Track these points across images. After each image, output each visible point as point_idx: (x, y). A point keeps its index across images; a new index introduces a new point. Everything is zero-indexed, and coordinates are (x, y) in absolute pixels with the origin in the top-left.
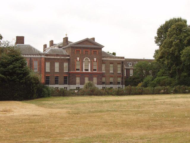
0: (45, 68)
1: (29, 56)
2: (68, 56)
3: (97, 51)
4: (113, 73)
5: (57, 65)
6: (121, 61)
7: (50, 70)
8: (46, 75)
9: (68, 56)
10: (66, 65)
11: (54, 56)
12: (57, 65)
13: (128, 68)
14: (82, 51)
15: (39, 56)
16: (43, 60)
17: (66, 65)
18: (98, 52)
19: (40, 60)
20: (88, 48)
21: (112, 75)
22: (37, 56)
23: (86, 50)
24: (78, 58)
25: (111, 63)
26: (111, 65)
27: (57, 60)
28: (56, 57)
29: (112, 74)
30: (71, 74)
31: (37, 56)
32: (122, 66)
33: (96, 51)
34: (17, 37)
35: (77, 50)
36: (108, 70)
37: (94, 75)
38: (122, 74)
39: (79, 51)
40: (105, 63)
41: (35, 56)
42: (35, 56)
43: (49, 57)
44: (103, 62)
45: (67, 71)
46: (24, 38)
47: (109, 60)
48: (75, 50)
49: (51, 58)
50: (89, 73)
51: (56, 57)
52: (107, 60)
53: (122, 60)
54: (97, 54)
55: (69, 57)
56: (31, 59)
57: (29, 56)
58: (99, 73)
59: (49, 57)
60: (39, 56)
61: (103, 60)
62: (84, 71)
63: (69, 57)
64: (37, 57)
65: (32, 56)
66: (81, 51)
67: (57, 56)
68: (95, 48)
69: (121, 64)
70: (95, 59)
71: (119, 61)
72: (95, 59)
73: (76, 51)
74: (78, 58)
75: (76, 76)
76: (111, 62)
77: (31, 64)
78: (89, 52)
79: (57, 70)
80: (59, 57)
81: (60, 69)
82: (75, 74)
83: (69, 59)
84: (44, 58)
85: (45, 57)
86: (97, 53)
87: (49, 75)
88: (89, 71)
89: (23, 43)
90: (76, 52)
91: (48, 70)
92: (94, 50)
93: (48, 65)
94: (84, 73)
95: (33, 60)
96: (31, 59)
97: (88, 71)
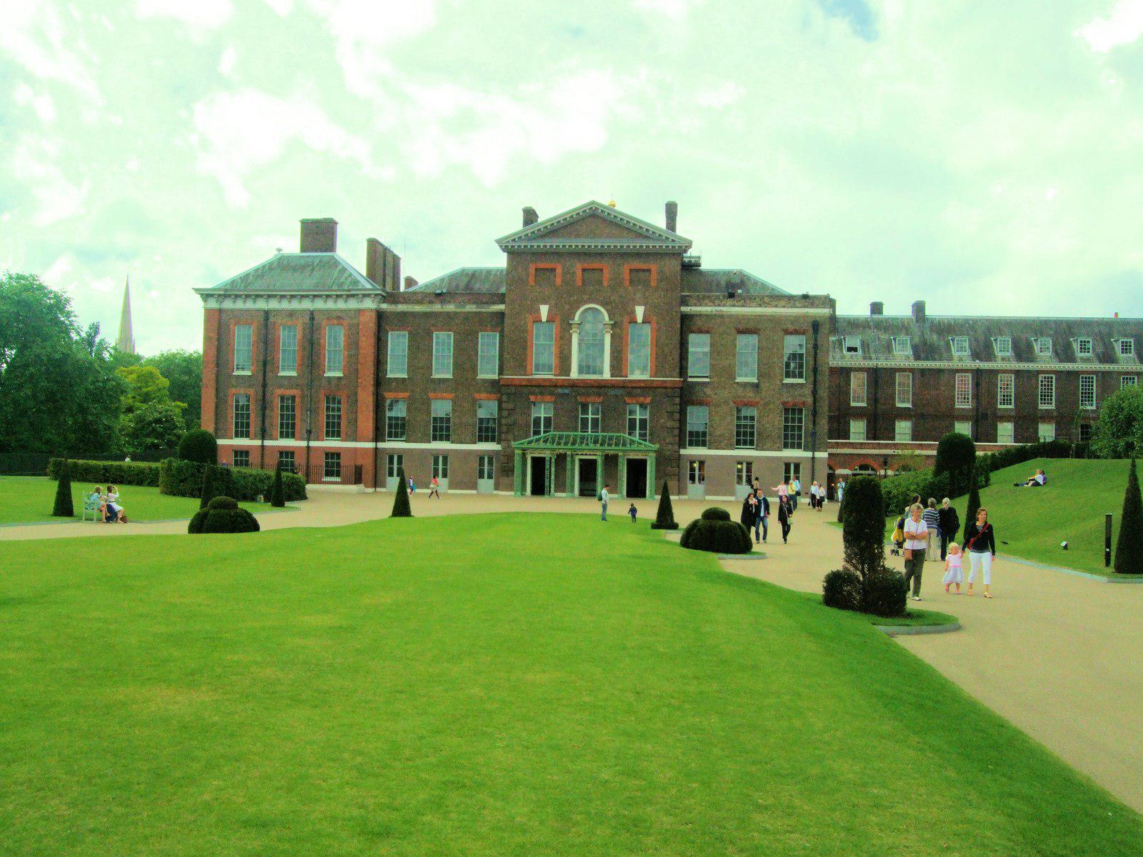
0: (379, 363)
1: (307, 305)
3: (654, 267)
4: (756, 386)
5: (443, 344)
6: (805, 317)
7: (412, 368)
9: (501, 299)
10: (488, 346)
11: (431, 302)
12: (443, 344)
13: (985, 365)
14: (565, 273)
15: (353, 304)
16: (369, 323)
17: (488, 346)
18: (661, 272)
19: (356, 321)
20: (600, 254)
21: (750, 394)
22: (341, 305)
23: (586, 266)
24: (544, 310)
25: (740, 332)
26: (747, 344)
27: (446, 321)
28: (437, 307)
29: (748, 389)
31: (341, 305)
32: (816, 347)
33: (644, 266)
35: (542, 265)
36: (724, 372)
37: (630, 395)
38: (814, 393)
39: (553, 270)
40: (707, 332)
41: (330, 305)
42: (330, 305)
43: (401, 308)
44: (687, 324)
45: (496, 377)
47: (730, 316)
48: (527, 269)
49: (413, 314)
50: (600, 386)
51: (437, 307)
52: (722, 316)
54: (653, 284)
55: (502, 307)
56: (312, 319)
57: (307, 305)
58: (663, 386)
59: (401, 308)
60: (353, 304)
61: (685, 318)
62: (574, 374)
63: (502, 307)
64: (341, 311)
65: (319, 305)
66: (559, 270)
67: (442, 302)
68: (638, 255)
69: (811, 331)
70: (640, 311)
71: (796, 319)
72: (640, 311)
73: (532, 271)
74: (544, 310)
75: (532, 398)
76: (747, 327)
77: (312, 344)
78: (606, 274)
79: (443, 369)
80: (450, 308)
81: (458, 366)
82: (525, 390)
83: (501, 315)
84: (374, 315)
85: (384, 306)
86: (654, 276)
88: (607, 375)
90: (531, 279)
91: (396, 369)
92: (637, 264)
94: (574, 385)
95: (324, 322)
96: (312, 319)
97: (601, 373)
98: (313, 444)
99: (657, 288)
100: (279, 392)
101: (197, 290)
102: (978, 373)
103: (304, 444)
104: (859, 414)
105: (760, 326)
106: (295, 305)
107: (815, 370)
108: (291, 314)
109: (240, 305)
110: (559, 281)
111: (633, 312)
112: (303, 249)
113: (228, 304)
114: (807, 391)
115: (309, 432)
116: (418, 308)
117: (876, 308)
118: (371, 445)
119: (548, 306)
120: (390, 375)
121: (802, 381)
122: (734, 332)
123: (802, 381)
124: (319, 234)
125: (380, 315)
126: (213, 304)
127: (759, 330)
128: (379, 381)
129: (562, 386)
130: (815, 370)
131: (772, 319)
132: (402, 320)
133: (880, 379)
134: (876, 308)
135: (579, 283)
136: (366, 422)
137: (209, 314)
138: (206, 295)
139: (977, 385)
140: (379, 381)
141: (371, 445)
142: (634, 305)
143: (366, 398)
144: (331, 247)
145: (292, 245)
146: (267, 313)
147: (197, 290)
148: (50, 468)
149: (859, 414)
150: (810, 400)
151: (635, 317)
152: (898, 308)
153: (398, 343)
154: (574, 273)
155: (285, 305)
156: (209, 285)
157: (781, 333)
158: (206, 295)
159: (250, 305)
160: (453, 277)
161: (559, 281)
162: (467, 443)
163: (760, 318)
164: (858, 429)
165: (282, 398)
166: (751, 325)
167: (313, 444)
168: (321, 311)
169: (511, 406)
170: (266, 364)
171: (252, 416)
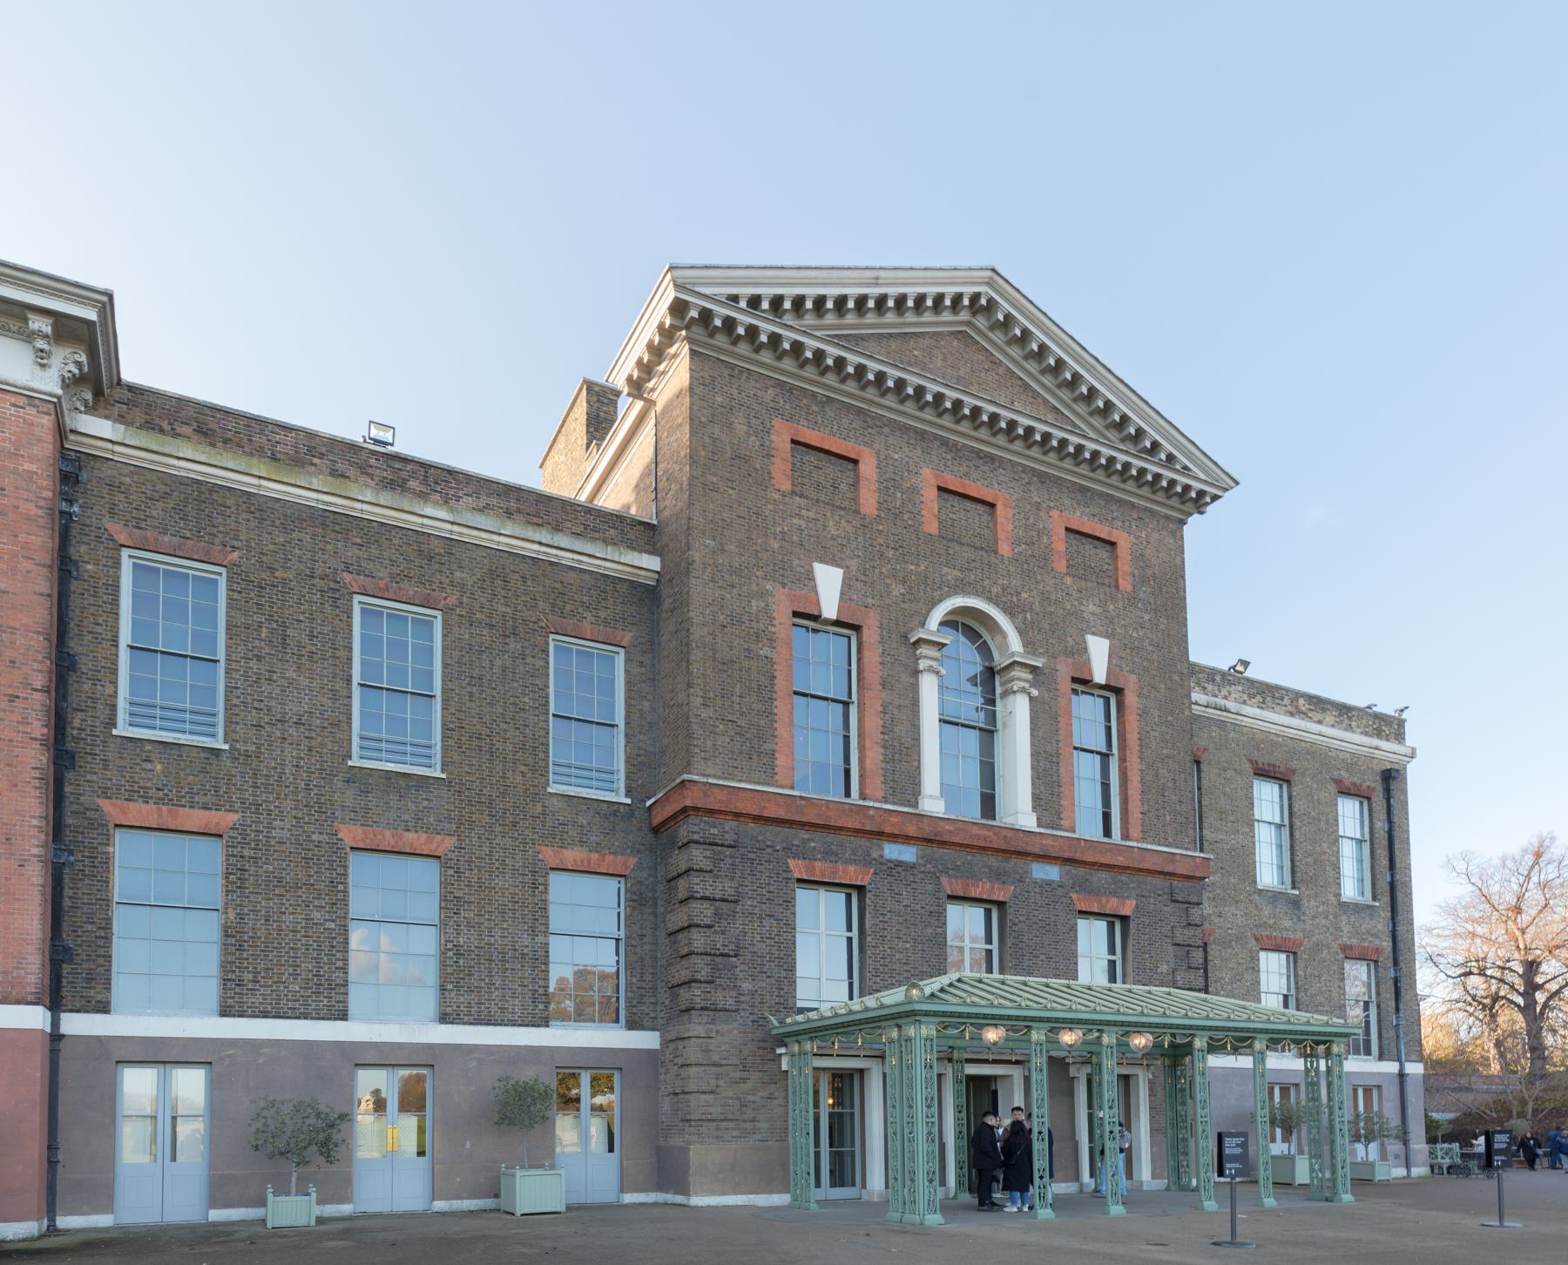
14: (888, 485)
18: (1139, 558)
30: (689, 829)
99: (1133, 599)
105: (1294, 764)
110: (869, 501)
111: (1084, 650)
114: (1381, 924)
119: (841, 571)
122: (1249, 768)
127: (1294, 772)
129: (894, 838)
135: (932, 527)
142: (1082, 633)
150: (1387, 945)
151: (1087, 664)
154: (915, 490)
157: (1332, 788)
161: (869, 501)
162: (513, 1024)
166: (1277, 758)
169: (724, 887)
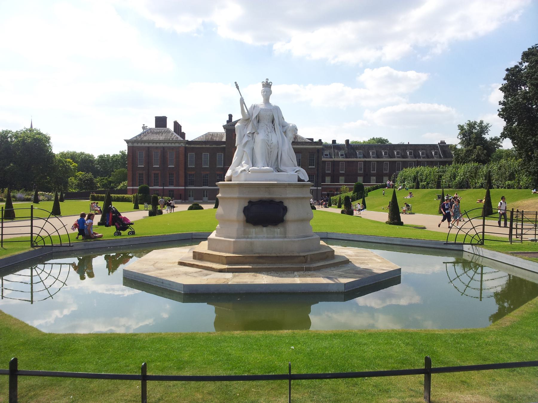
2: (224, 143)
6: (315, 148)
8: (189, 173)
22: (173, 145)
27: (207, 150)
34: (156, 117)
38: (318, 170)
43: (192, 146)
46: (167, 119)
51: (204, 146)
53: (317, 146)
59: (192, 146)
60: (177, 145)
71: (313, 148)
80: (208, 146)
83: (224, 148)
85: (187, 145)
87: (193, 173)
89: (166, 127)
93: (191, 156)
98: (165, 188)
100: (154, 172)
101: (125, 140)
102: (365, 162)
103: (162, 188)
104: (328, 175)
106: (158, 145)
107: (318, 163)
108: (157, 148)
109: (139, 145)
112: (156, 127)
113: (135, 145)
115: (164, 184)
116: (197, 146)
117: (334, 142)
118: (184, 188)
120: (189, 166)
121: (314, 167)
123: (314, 167)
124: (161, 121)
125: (186, 148)
126: (130, 145)
128: (186, 168)
130: (318, 163)
131: (305, 149)
132: (193, 149)
133: (335, 164)
134: (334, 142)
136: (182, 180)
137: (128, 147)
138: (128, 142)
139: (365, 165)
140: (186, 168)
141: (184, 188)
143: (182, 173)
144: (165, 126)
145: (152, 125)
146: (149, 147)
147: (125, 140)
148: (91, 197)
149: (328, 175)
150: (316, 172)
152: (341, 141)
153: (191, 156)
155: (155, 145)
156: (129, 138)
158: (128, 142)
159: (143, 145)
160: (206, 135)
163: (302, 149)
164: (328, 179)
165: (154, 174)
167: (165, 188)
168: (166, 147)
170: (149, 163)
171: (144, 180)
